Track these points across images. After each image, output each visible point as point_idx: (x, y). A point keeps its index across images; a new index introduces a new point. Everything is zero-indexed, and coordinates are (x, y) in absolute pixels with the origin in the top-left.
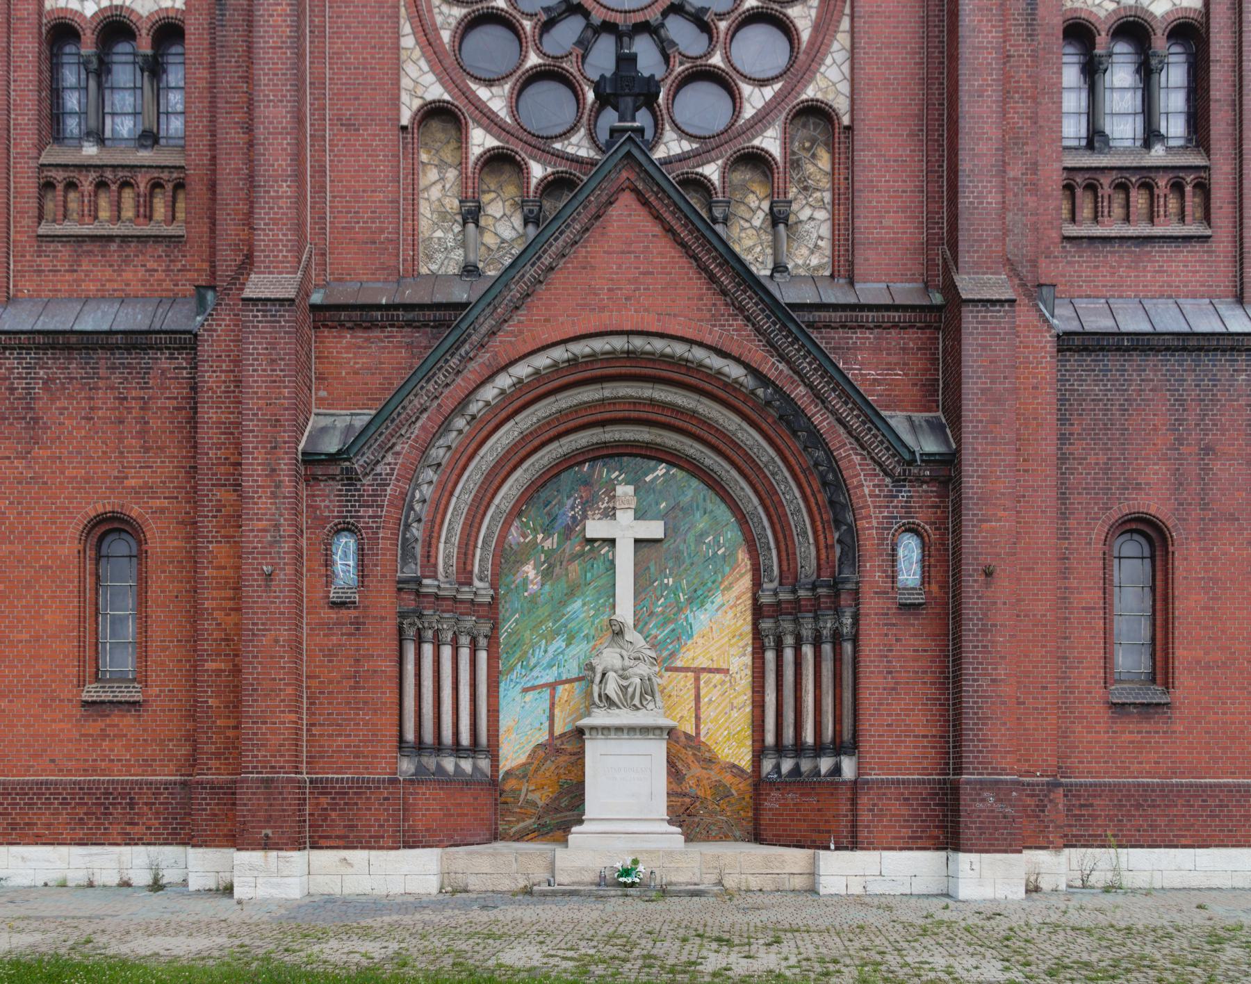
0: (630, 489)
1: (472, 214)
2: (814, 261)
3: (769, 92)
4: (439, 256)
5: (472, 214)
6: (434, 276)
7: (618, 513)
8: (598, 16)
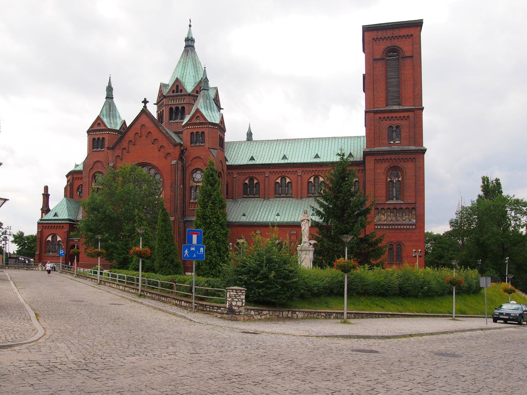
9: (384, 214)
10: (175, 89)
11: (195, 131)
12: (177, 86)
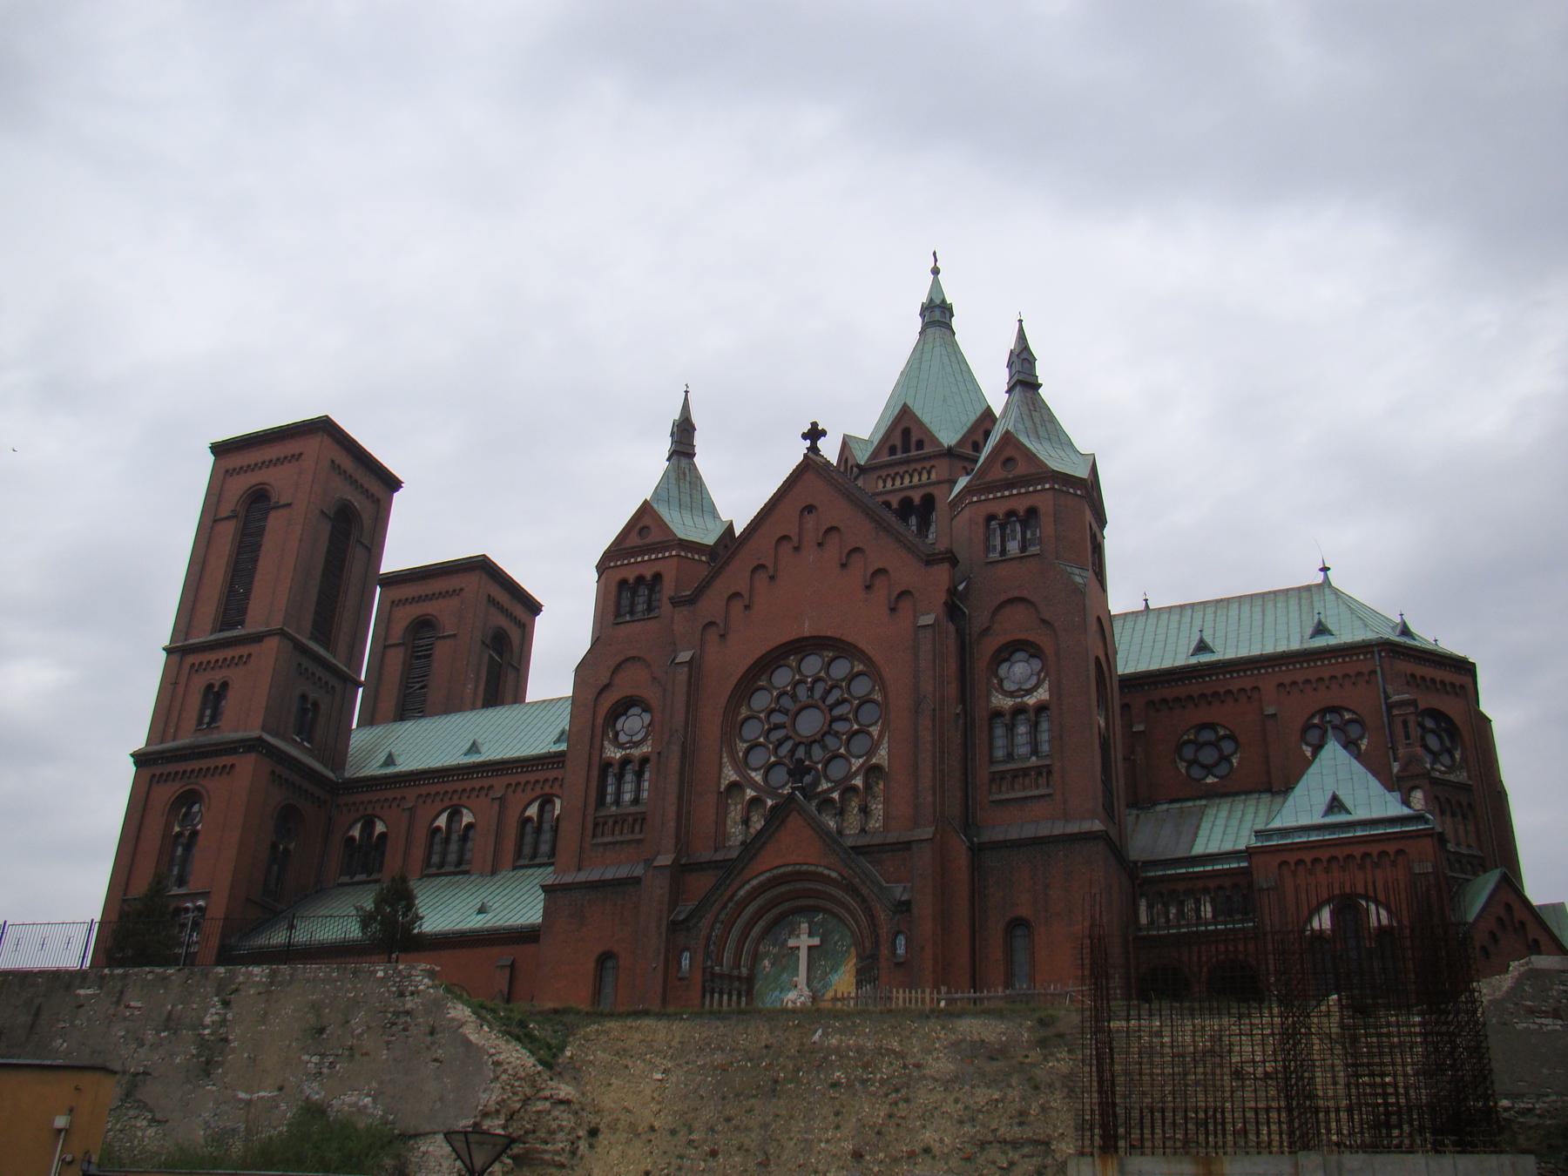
0: (807, 925)
1: (746, 822)
2: (877, 825)
3: (861, 760)
4: (733, 839)
5: (746, 822)
6: (730, 847)
7: (801, 936)
8: (798, 739)
10: (898, 443)
12: (906, 433)
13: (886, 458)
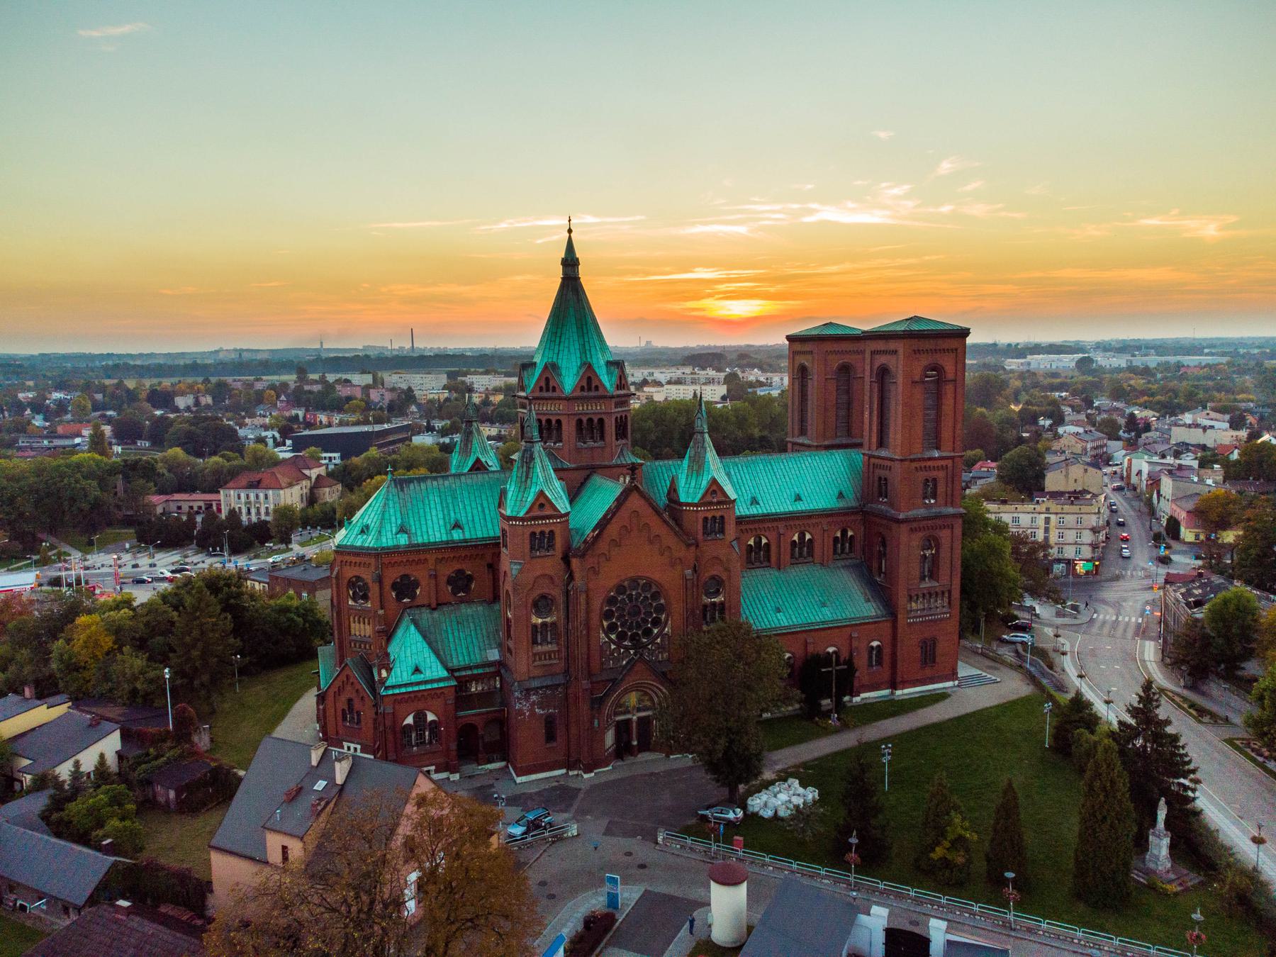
9: (916, 602)
11: (709, 515)
12: (589, 378)
13: (578, 393)
